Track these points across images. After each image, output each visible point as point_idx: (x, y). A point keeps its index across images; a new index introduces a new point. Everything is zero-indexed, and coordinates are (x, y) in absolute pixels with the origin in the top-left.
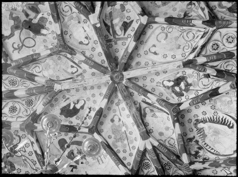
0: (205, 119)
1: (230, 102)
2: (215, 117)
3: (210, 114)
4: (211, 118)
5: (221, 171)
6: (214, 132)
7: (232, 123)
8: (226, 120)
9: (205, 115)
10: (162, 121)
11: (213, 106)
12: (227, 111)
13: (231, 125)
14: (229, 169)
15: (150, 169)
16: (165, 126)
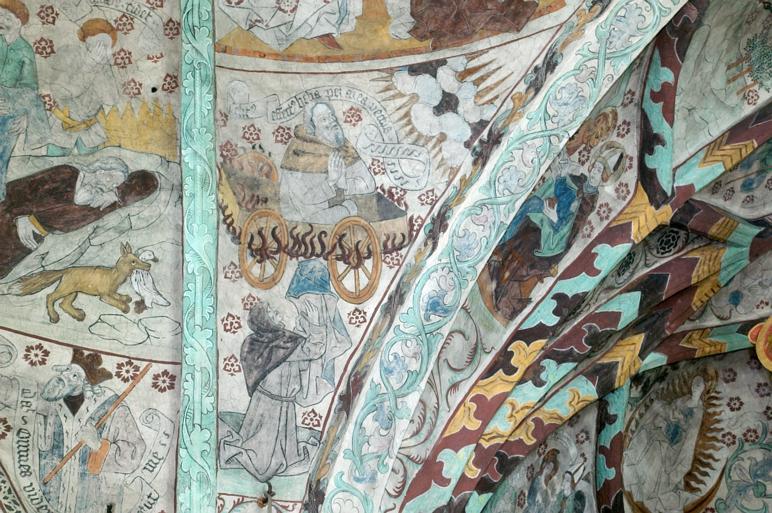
0: (714, 402)
1: (761, 489)
2: (719, 437)
3: (726, 417)
4: (718, 421)
5: (583, 455)
6: (677, 427)
7: (701, 486)
8: (707, 470)
9: (729, 405)
10: (760, 284)
11: (757, 437)
12: (735, 476)
13: (693, 483)
14: (586, 479)
15: (655, 252)
16: (745, 292)
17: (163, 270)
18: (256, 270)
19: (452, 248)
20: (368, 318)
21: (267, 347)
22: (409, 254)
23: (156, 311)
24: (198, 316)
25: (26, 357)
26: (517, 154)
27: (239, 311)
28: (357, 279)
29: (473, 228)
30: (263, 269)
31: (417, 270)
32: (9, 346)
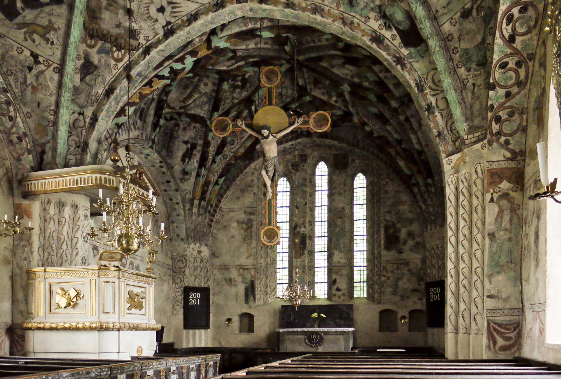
17: (61, 33)
18: (89, 42)
19: (149, 60)
20: (119, 68)
21: (88, 68)
22: (136, 54)
23: (57, 46)
24: (71, 57)
25: (17, 50)
26: (176, 40)
27: (81, 54)
28: (118, 54)
29: (157, 56)
30: (91, 42)
31: (137, 63)
32: (12, 46)
